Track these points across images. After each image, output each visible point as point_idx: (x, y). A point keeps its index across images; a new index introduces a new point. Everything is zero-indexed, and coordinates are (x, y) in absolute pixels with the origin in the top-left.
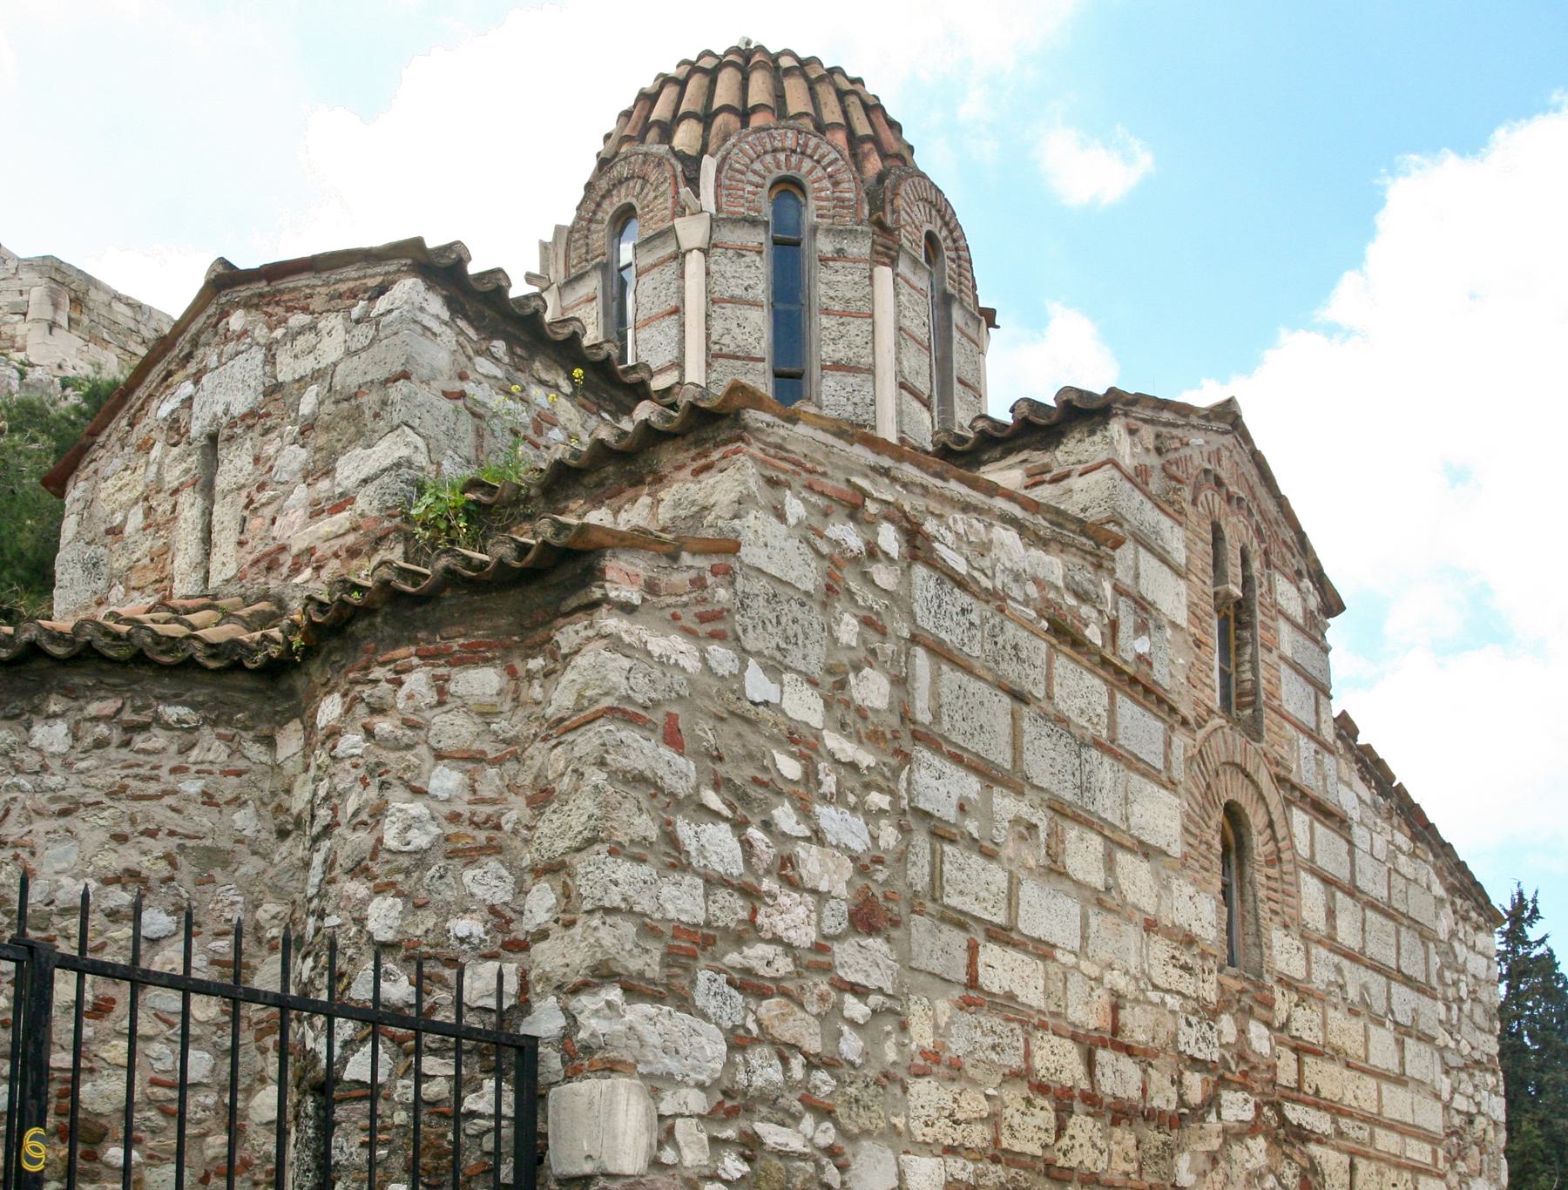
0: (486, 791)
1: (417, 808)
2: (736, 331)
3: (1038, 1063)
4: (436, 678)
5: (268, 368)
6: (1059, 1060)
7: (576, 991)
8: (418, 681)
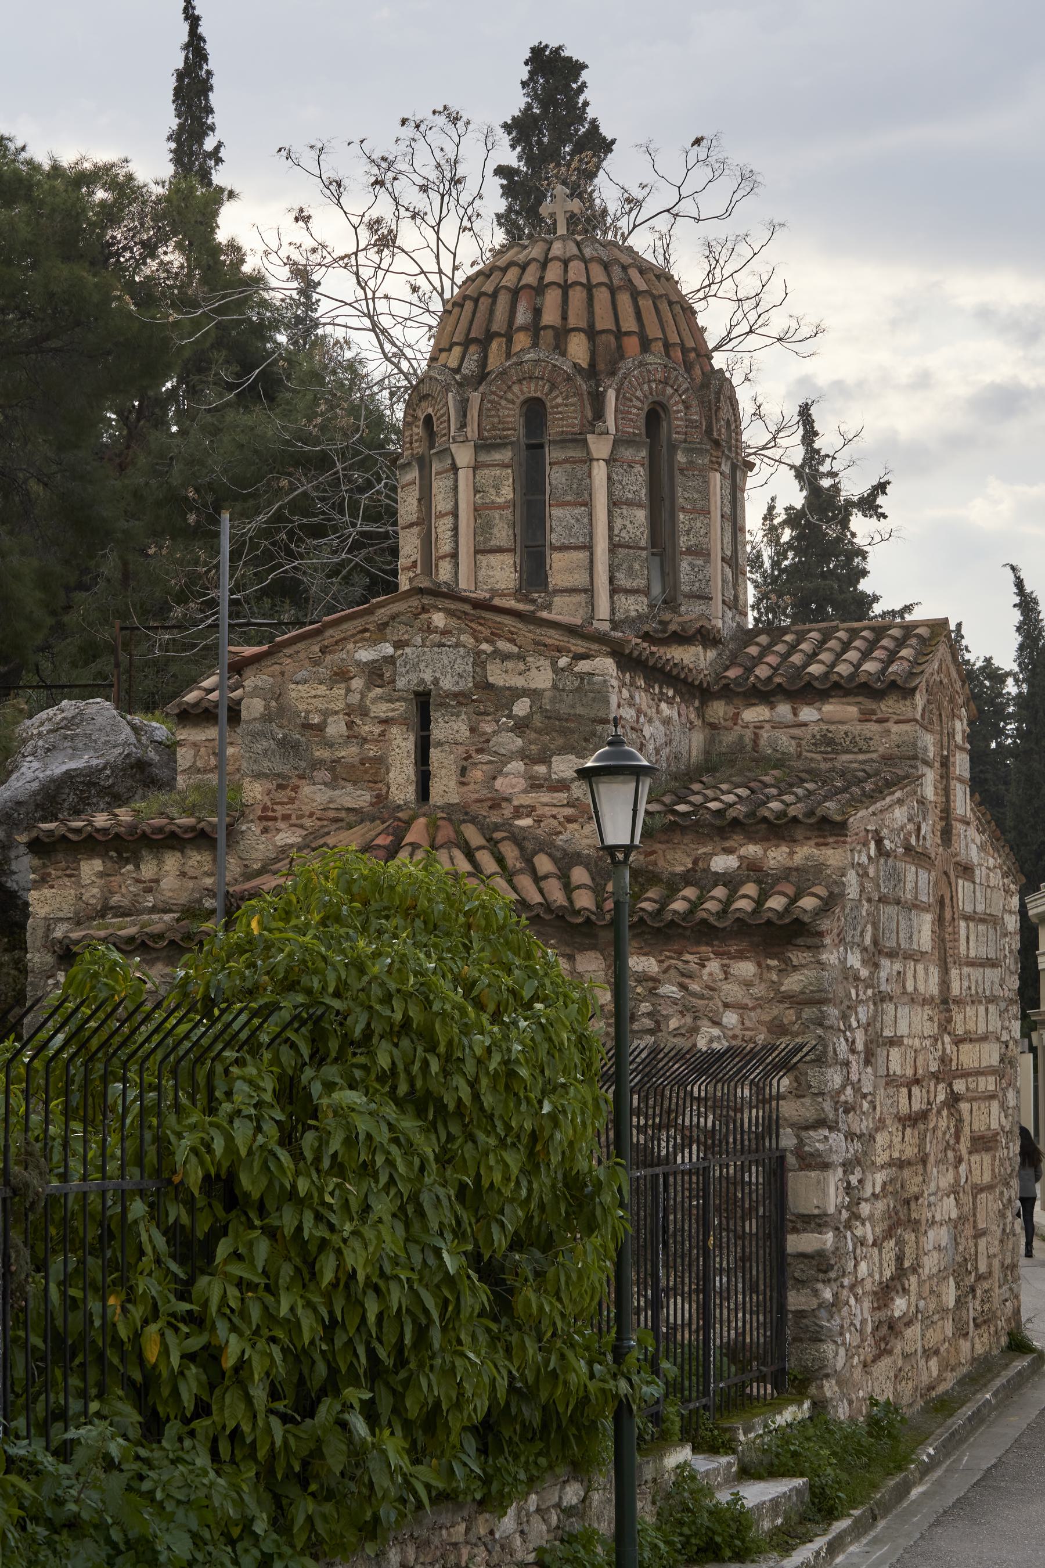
0: (748, 1024)
1: (716, 1032)
2: (629, 525)
4: (723, 965)
5: (478, 669)
7: (807, 1128)
8: (714, 966)
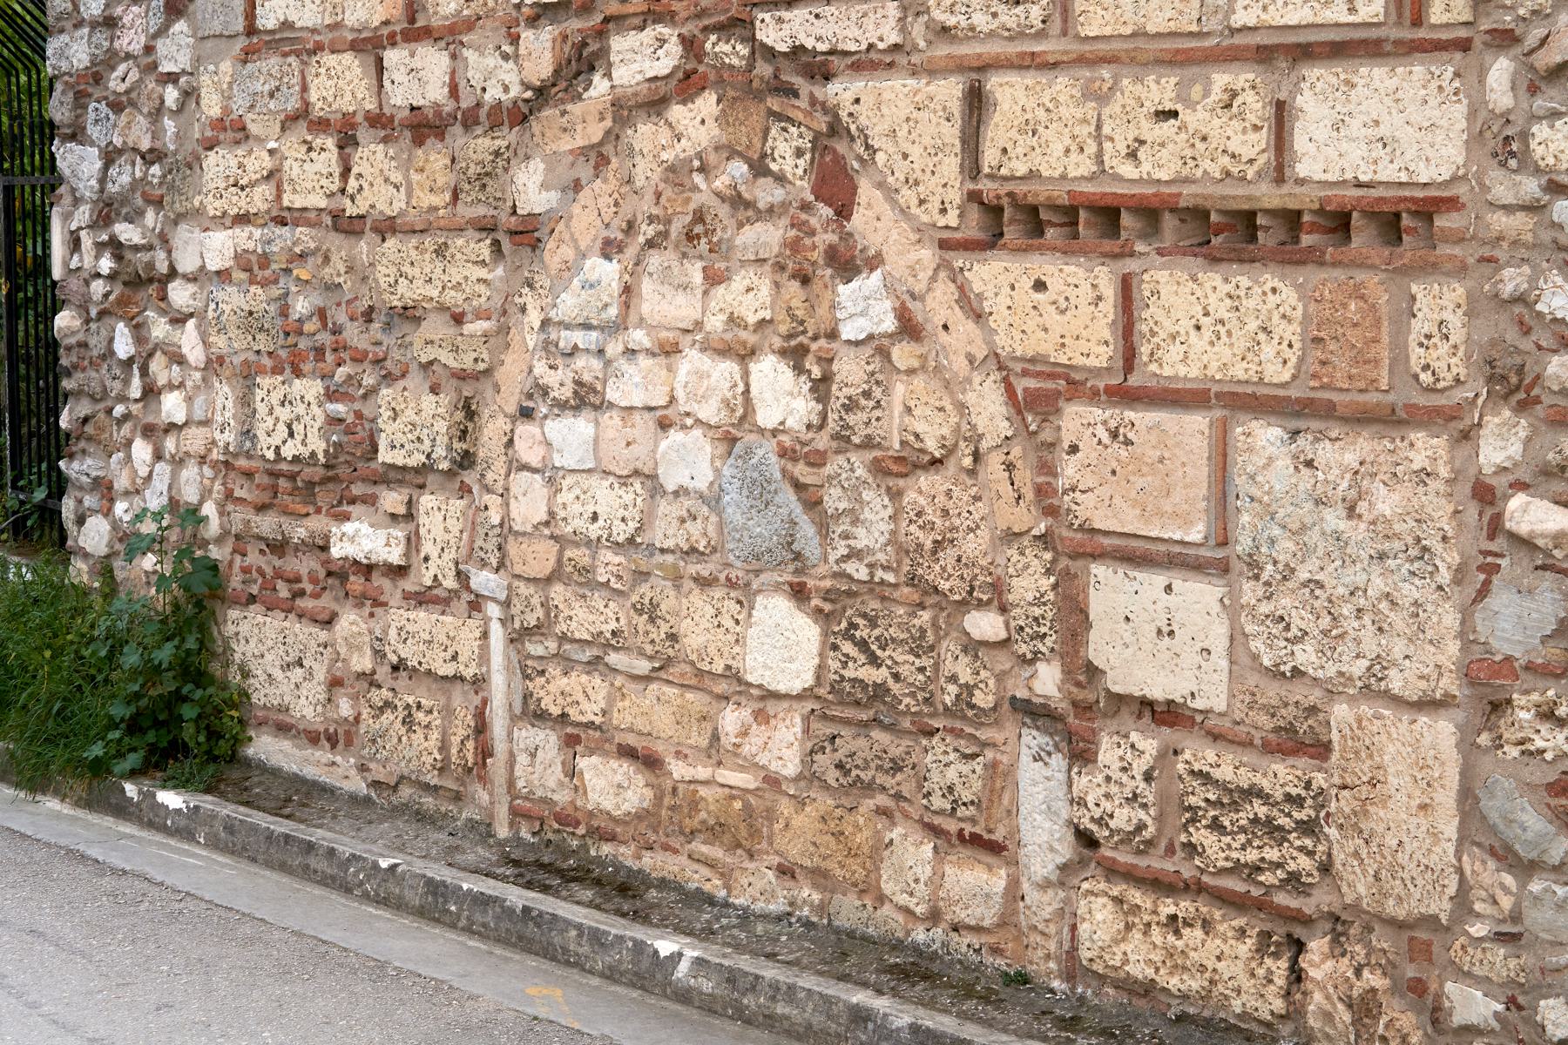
3: (313, 96)
6: (340, 83)
